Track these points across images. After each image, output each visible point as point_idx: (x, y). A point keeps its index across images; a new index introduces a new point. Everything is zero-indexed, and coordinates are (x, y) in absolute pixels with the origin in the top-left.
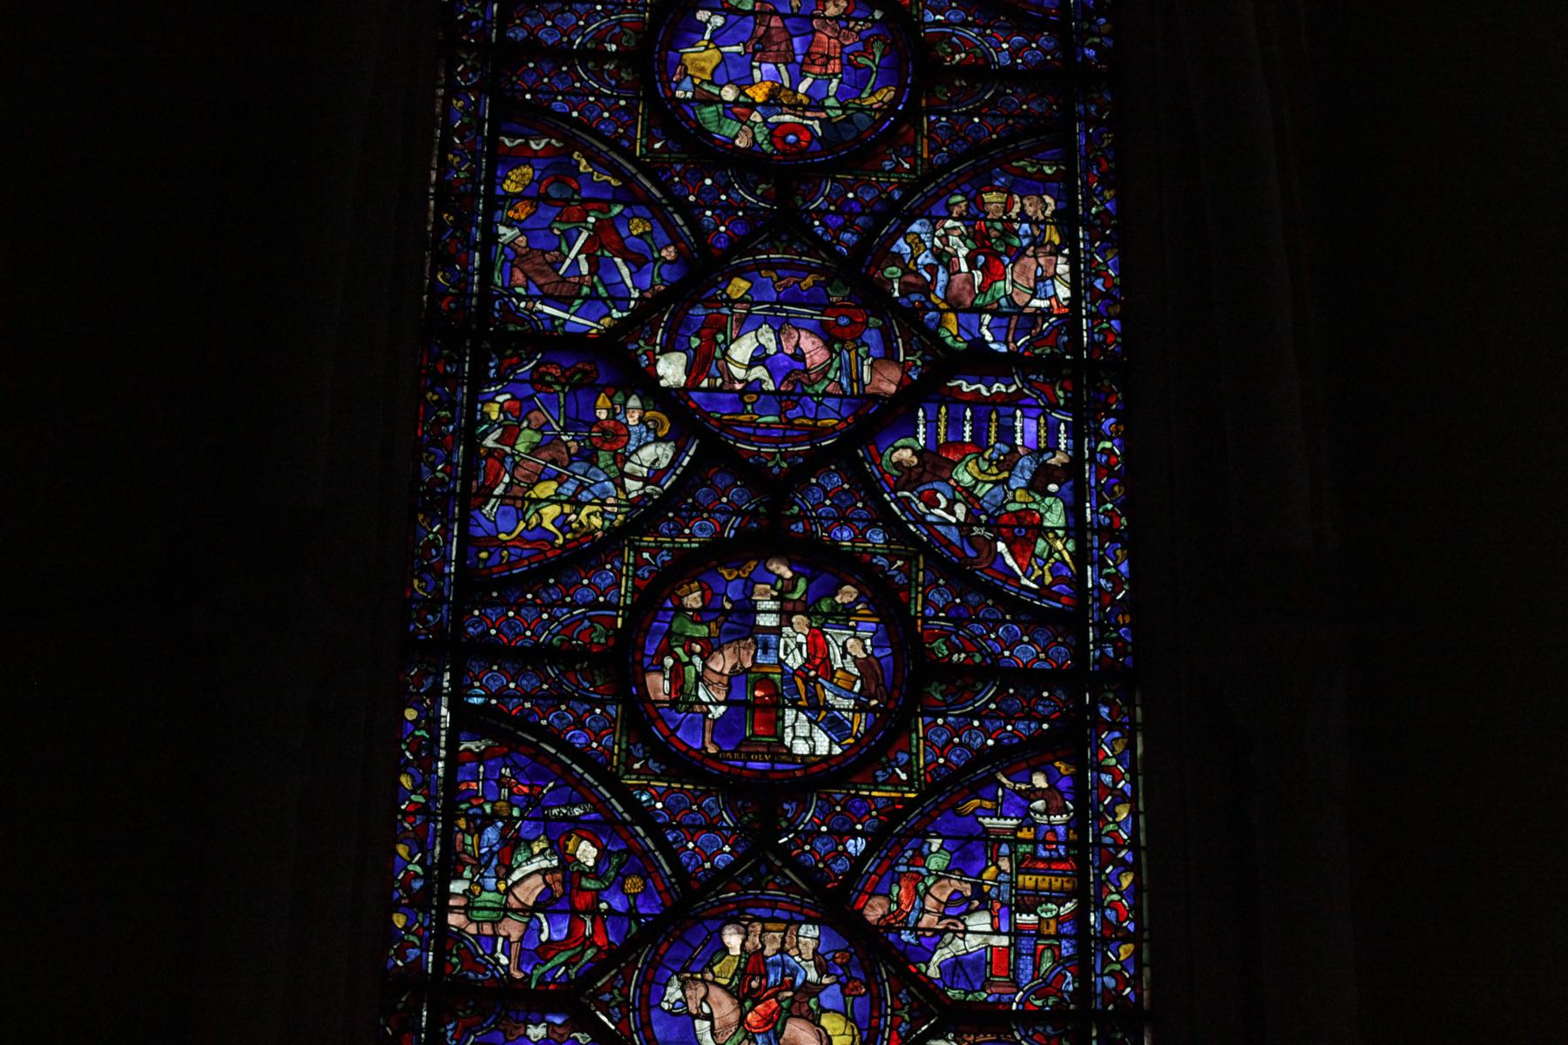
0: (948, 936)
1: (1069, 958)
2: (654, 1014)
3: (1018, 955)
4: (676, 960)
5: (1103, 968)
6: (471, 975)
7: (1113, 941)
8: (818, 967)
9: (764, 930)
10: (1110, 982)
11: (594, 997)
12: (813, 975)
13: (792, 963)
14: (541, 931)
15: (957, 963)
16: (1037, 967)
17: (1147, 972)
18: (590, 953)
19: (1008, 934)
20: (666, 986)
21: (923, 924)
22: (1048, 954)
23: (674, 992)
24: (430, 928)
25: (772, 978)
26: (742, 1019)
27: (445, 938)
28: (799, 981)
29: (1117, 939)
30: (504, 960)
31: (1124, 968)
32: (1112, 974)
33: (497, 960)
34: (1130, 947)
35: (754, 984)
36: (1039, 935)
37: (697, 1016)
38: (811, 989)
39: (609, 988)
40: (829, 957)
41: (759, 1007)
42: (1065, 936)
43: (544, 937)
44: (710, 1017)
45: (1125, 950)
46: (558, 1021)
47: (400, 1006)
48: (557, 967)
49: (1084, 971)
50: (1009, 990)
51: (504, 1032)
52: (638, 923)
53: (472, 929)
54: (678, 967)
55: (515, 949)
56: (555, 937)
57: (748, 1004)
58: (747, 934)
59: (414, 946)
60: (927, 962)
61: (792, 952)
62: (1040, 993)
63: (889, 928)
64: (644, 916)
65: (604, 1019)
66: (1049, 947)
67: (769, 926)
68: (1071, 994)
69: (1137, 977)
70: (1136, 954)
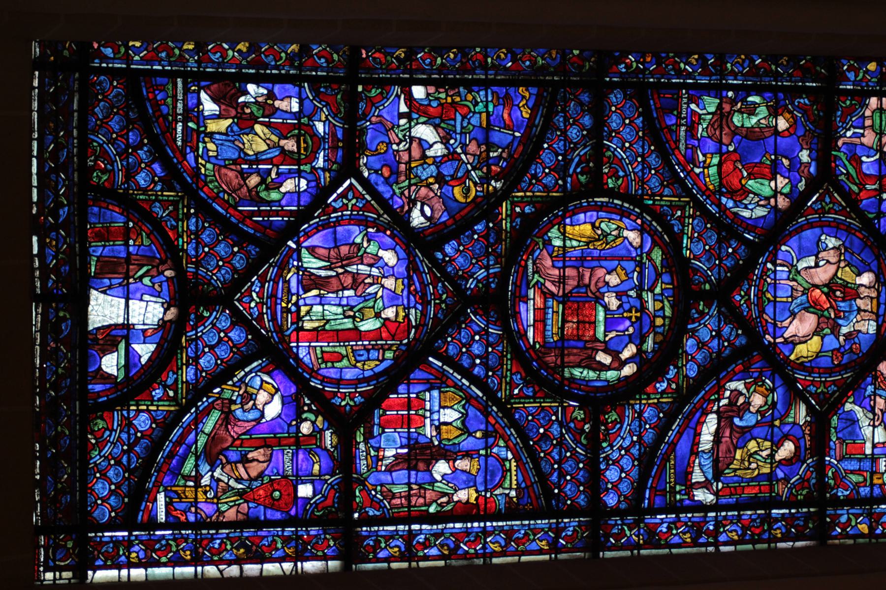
0: (871, 416)
1: (858, 493)
2: (817, 230)
3: (860, 460)
4: (851, 243)
5: (853, 514)
6: (839, 113)
7: (870, 520)
8: (850, 333)
9: (872, 298)
10: (843, 519)
11: (827, 192)
12: (844, 330)
13: (852, 317)
14: (868, 157)
15: (853, 421)
16: (853, 472)
17: (851, 542)
18: (855, 188)
19: (873, 454)
20: (836, 237)
21: (878, 399)
22: (861, 479)
23: (832, 242)
24: (868, 86)
25: (842, 304)
26: (816, 286)
27: (862, 96)
28: (840, 322)
29: (871, 523)
30: (849, 134)
31: (853, 527)
32: (849, 520)
33: (849, 129)
34: (866, 531)
35: (838, 293)
36: (873, 473)
37: (817, 257)
38: (835, 329)
39: (833, 201)
40: (856, 340)
41: (824, 297)
42: (872, 490)
43: (864, 159)
44: (817, 265)
45: (864, 528)
46: (812, 170)
47: (818, 68)
48: (845, 167)
49: (850, 502)
50: (838, 454)
51: (804, 135)
52: (875, 218)
53: (868, 113)
54: (847, 244)
55: (856, 141)
56: (864, 166)
57: (825, 290)
58: (869, 288)
59: (856, 76)
60: (854, 402)
61: (859, 317)
62: (835, 476)
63: (875, 378)
64: (879, 222)
65: (814, 199)
66: (865, 479)
67: (875, 302)
68: (836, 494)
69: (848, 536)
70: (862, 535)
